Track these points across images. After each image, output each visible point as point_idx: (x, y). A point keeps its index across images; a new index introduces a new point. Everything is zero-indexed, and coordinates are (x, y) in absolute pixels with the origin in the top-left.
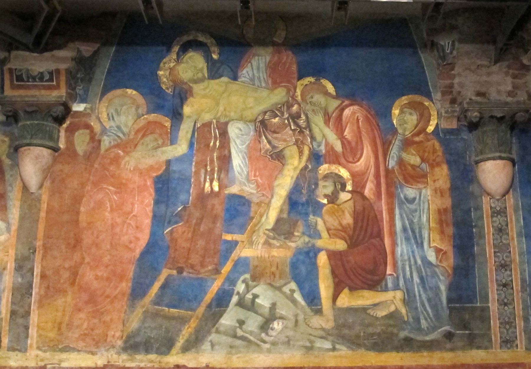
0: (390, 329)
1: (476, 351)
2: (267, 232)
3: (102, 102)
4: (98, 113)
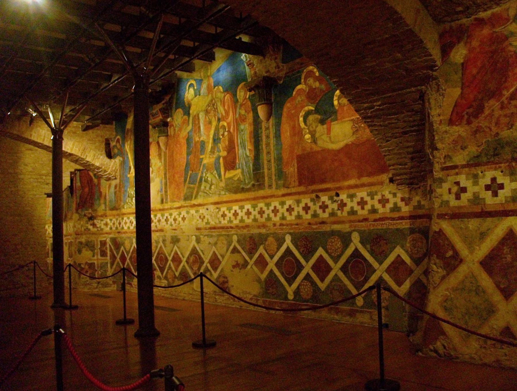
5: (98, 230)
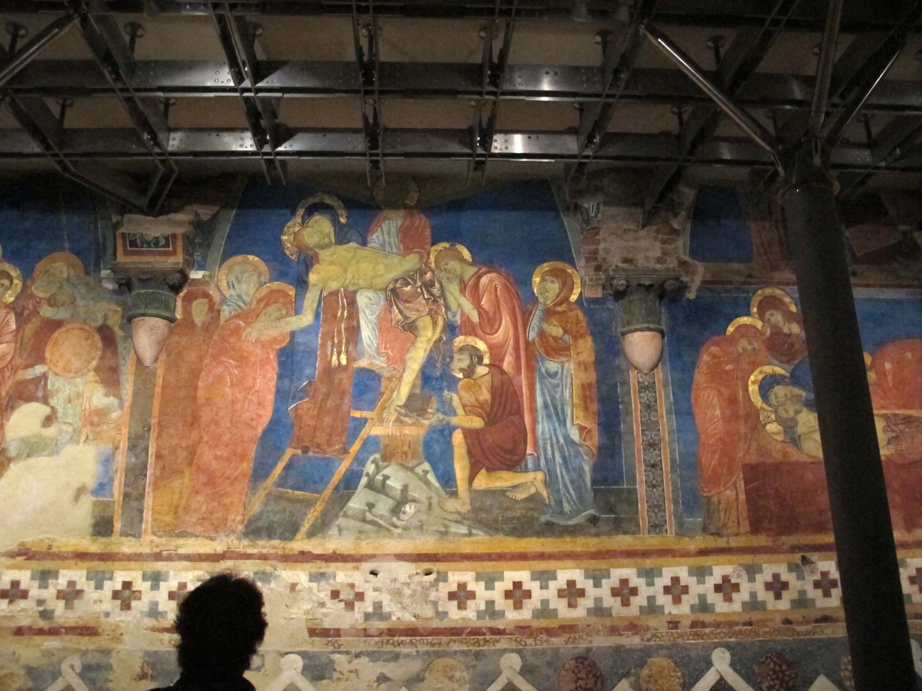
0: (530, 513)
1: (623, 536)
2: (398, 409)
3: (221, 269)
4: (218, 281)
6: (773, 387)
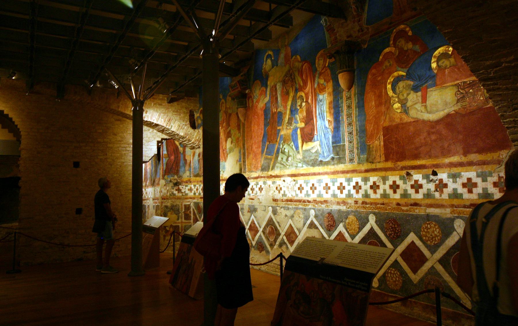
5: (183, 195)
6: (398, 84)
